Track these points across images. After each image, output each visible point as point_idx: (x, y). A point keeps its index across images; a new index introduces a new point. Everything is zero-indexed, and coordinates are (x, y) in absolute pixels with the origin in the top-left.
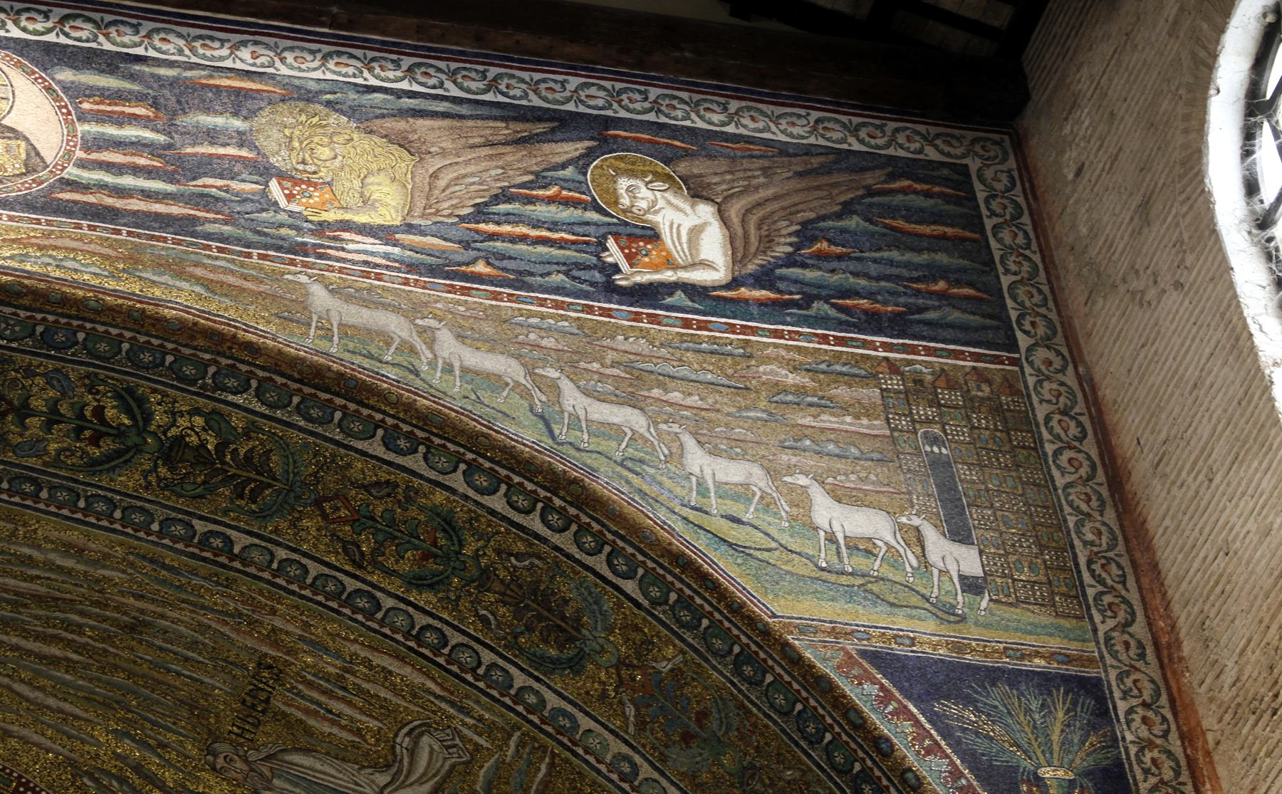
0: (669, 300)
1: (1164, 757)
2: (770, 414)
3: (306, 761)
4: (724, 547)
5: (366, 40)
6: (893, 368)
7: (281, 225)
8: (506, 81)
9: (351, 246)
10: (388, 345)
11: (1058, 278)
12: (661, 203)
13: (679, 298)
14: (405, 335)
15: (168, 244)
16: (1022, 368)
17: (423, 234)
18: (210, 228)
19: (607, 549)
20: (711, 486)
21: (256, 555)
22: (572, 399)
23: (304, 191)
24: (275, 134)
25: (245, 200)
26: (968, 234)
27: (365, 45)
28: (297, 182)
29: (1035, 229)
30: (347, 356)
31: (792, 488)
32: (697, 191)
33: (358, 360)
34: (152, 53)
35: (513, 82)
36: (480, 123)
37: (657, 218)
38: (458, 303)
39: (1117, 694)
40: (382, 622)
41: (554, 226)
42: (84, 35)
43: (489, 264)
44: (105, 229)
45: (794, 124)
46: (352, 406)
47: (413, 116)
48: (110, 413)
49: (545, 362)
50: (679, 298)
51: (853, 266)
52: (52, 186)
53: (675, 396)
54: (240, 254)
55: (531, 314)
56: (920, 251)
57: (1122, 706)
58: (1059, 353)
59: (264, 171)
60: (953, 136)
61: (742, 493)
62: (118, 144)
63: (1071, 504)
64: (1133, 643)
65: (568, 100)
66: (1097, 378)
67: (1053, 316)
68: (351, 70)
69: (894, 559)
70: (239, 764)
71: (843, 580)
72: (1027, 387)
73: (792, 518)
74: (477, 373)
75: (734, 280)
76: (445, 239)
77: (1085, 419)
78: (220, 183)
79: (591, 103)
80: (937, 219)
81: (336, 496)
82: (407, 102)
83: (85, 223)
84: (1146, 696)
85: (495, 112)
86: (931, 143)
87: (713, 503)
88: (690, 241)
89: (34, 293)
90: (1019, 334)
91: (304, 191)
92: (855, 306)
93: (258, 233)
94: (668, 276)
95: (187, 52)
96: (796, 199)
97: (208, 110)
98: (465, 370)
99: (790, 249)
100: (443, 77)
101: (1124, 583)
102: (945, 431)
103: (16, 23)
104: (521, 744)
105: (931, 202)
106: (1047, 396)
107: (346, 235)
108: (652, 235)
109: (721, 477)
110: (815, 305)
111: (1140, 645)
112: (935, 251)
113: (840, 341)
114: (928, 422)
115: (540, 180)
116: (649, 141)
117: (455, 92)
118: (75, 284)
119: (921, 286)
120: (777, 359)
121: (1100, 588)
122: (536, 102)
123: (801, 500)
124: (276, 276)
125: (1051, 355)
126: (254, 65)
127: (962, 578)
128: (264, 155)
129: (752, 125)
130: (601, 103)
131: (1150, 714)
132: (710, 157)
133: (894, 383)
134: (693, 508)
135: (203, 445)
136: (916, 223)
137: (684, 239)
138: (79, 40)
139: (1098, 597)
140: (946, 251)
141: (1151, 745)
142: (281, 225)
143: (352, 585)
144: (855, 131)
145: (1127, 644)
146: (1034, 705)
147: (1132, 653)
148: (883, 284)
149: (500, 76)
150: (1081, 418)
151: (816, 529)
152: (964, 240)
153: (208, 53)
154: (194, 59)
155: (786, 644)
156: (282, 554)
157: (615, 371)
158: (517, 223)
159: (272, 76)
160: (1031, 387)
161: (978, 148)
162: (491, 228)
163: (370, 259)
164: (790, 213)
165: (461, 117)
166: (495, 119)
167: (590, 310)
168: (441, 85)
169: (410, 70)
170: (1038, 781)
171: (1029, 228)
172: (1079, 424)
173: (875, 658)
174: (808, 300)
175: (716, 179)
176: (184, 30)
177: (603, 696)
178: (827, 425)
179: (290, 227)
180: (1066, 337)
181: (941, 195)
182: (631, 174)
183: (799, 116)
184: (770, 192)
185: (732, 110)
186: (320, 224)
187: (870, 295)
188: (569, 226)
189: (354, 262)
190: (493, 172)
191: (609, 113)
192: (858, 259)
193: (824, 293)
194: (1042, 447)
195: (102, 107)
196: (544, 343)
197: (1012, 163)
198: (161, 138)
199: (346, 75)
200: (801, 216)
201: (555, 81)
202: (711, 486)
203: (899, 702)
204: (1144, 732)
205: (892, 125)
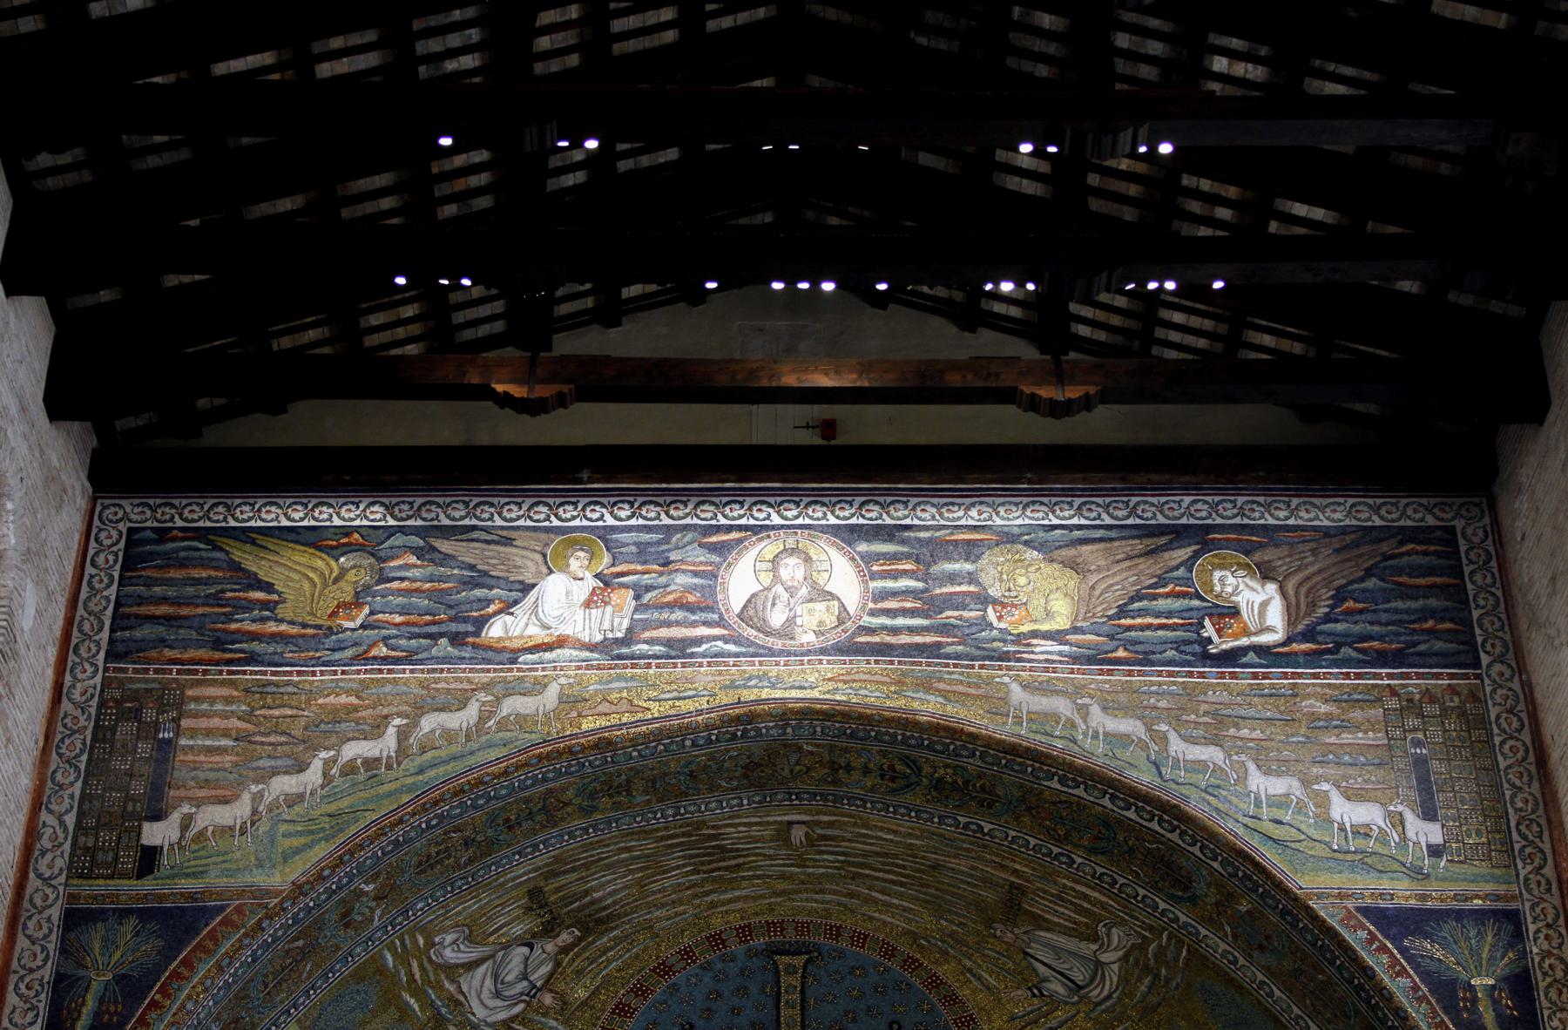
0: (1244, 660)
1: (1558, 962)
2: (1308, 737)
3: (1048, 935)
4: (1271, 842)
5: (1051, 489)
6: (1393, 692)
7: (994, 640)
8: (1142, 507)
9: (1037, 649)
10: (1058, 723)
11: (1513, 606)
12: (1242, 587)
13: (1251, 657)
14: (1068, 714)
15: (924, 666)
16: (1482, 681)
17: (1084, 633)
18: (949, 649)
19: (1199, 844)
20: (1263, 796)
21: (997, 834)
22: (1176, 746)
23: (1009, 612)
24: (993, 572)
25: (971, 625)
26: (1452, 581)
27: (1051, 493)
28: (1004, 605)
29: (1500, 570)
30: (1031, 735)
31: (1317, 793)
32: (1266, 575)
33: (1039, 737)
34: (916, 522)
35: (1147, 507)
36: (1123, 542)
37: (1239, 599)
38: (1105, 682)
39: (1529, 920)
40: (1077, 869)
41: (1169, 614)
42: (873, 515)
43: (1126, 649)
44: (884, 661)
45: (1335, 511)
46: (1037, 765)
47: (1080, 544)
48: (898, 767)
49: (1159, 719)
50: (1251, 657)
51: (1369, 617)
52: (854, 633)
53: (1245, 732)
54: (967, 667)
55: (1152, 684)
56: (1417, 599)
57: (1532, 928)
58: (1509, 666)
59: (984, 600)
60: (1446, 504)
61: (1281, 802)
62: (894, 594)
63: (1508, 781)
64: (1543, 882)
65: (1182, 515)
66: (1534, 682)
67: (1508, 637)
68: (1040, 515)
69: (1383, 838)
70: (1009, 935)
71: (1349, 857)
72: (1485, 695)
73: (1317, 816)
74: (1114, 735)
75: (1289, 638)
76: (1098, 635)
77: (1524, 715)
78: (956, 613)
79: (1198, 515)
80: (1431, 571)
81: (1038, 807)
82: (1077, 534)
83: (872, 658)
84: (1550, 920)
85: (1134, 532)
86: (1430, 512)
87: (1265, 812)
88: (1260, 613)
89: (843, 714)
90: (1483, 655)
91: (1009, 612)
92: (1370, 647)
93: (979, 648)
94: (1244, 641)
95: (938, 517)
96: (1333, 570)
97: (950, 559)
98: (1106, 734)
99: (1327, 610)
100: (1101, 510)
101: (1540, 837)
102: (1425, 735)
103: (833, 513)
104: (1169, 938)
105: (1427, 559)
106: (1499, 700)
107: (1035, 641)
108: (1234, 612)
109: (1271, 791)
110: (1343, 650)
111: (1549, 883)
112: (1428, 597)
113: (1358, 676)
114: (1415, 730)
115: (1161, 581)
116: (1235, 539)
117: (1108, 521)
118: (867, 706)
119: (1416, 626)
120: (1314, 695)
121: (1524, 843)
122: (1162, 520)
123: (1323, 801)
124: (989, 682)
125: (1503, 668)
126: (979, 520)
127: (1429, 846)
128: (985, 589)
129: (1306, 516)
130: (1204, 514)
131: (1551, 932)
132: (1277, 546)
133: (1393, 704)
134: (1252, 817)
135: (955, 782)
136: (1417, 577)
137: (1256, 612)
138: (871, 519)
139: (1523, 848)
140: (1436, 596)
141: (1549, 954)
142: (994, 640)
143: (1056, 850)
144: (1376, 510)
145: (1539, 883)
146: (1472, 933)
147: (1542, 889)
148: (1390, 628)
149: (1138, 503)
150: (1521, 714)
151: (1332, 822)
152: (1448, 585)
153: (951, 516)
154: (943, 522)
155: (1308, 908)
156: (1014, 833)
157: (1206, 719)
158: (1145, 616)
159: (990, 527)
160: (1488, 692)
161: (1463, 512)
162: (1128, 621)
163: (1049, 657)
164: (1328, 582)
165: (1111, 540)
166: (1134, 537)
167: (1190, 674)
168: (1099, 517)
169: (1079, 508)
170: (1471, 988)
171: (1495, 570)
172: (1520, 719)
173: (1365, 911)
174: (1338, 646)
175: (1280, 563)
176: (935, 500)
177: (1211, 918)
178: (1345, 741)
179: (999, 640)
180: (1515, 653)
181: (1436, 553)
182: (1222, 567)
183: (1339, 504)
184: (1316, 568)
185: (1293, 506)
186: (1019, 635)
187: (1381, 638)
188: (1179, 613)
189: (1039, 661)
190: (1131, 580)
191: (1209, 521)
192: (1374, 611)
193: (1349, 640)
194: (1492, 739)
195: (885, 568)
196: (1160, 705)
197: (1487, 520)
198: (920, 585)
199: (1038, 519)
200: (1337, 583)
201: (1174, 502)
202: (1263, 796)
203: (1380, 941)
204: (1545, 946)
205: (1404, 501)
